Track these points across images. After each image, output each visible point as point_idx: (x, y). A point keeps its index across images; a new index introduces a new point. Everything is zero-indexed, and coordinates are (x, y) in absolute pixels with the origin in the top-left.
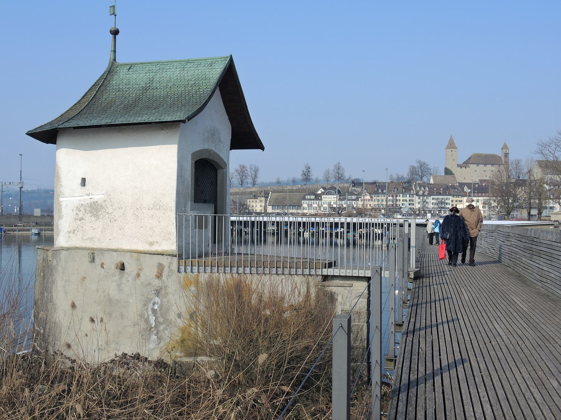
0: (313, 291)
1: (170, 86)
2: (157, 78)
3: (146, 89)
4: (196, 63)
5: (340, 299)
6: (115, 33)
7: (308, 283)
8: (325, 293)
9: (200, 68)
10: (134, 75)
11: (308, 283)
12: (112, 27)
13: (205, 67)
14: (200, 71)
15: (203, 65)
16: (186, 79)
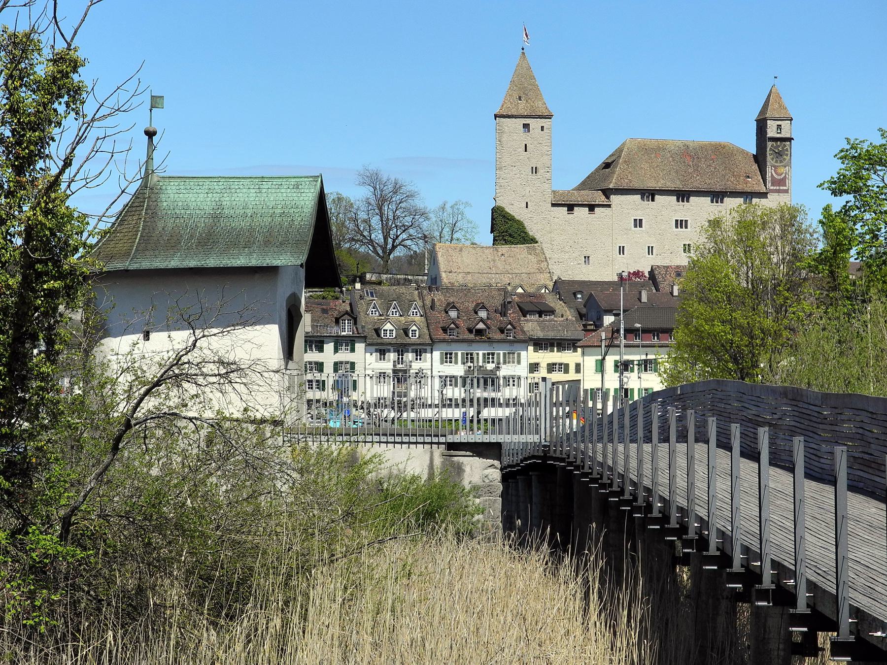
0: (438, 461)
1: (250, 214)
2: (226, 201)
3: (216, 217)
4: (274, 183)
5: (467, 469)
6: (150, 134)
7: (432, 453)
8: (453, 464)
9: (283, 191)
10: (191, 195)
11: (432, 453)
12: (146, 125)
13: (289, 190)
14: (285, 195)
15: (285, 187)
16: (268, 206)
